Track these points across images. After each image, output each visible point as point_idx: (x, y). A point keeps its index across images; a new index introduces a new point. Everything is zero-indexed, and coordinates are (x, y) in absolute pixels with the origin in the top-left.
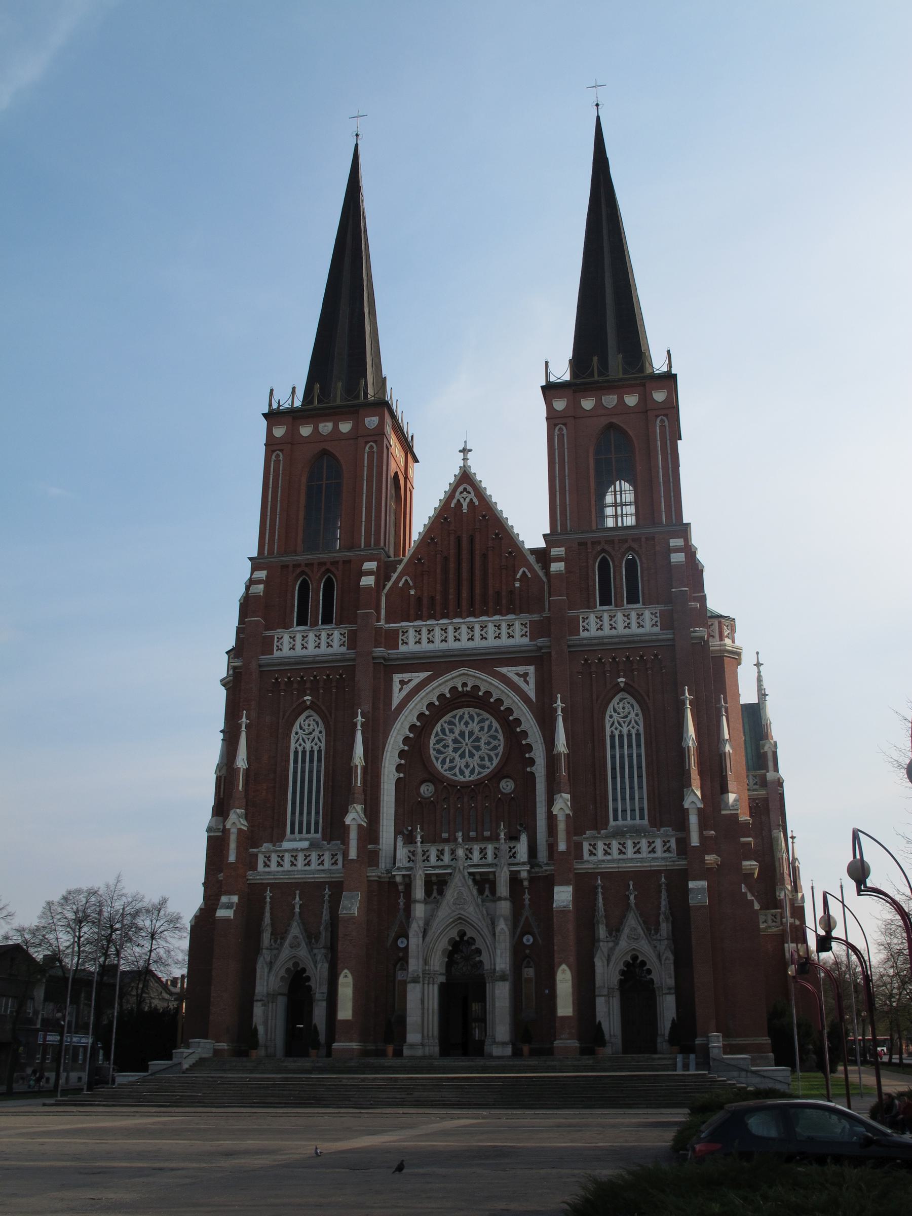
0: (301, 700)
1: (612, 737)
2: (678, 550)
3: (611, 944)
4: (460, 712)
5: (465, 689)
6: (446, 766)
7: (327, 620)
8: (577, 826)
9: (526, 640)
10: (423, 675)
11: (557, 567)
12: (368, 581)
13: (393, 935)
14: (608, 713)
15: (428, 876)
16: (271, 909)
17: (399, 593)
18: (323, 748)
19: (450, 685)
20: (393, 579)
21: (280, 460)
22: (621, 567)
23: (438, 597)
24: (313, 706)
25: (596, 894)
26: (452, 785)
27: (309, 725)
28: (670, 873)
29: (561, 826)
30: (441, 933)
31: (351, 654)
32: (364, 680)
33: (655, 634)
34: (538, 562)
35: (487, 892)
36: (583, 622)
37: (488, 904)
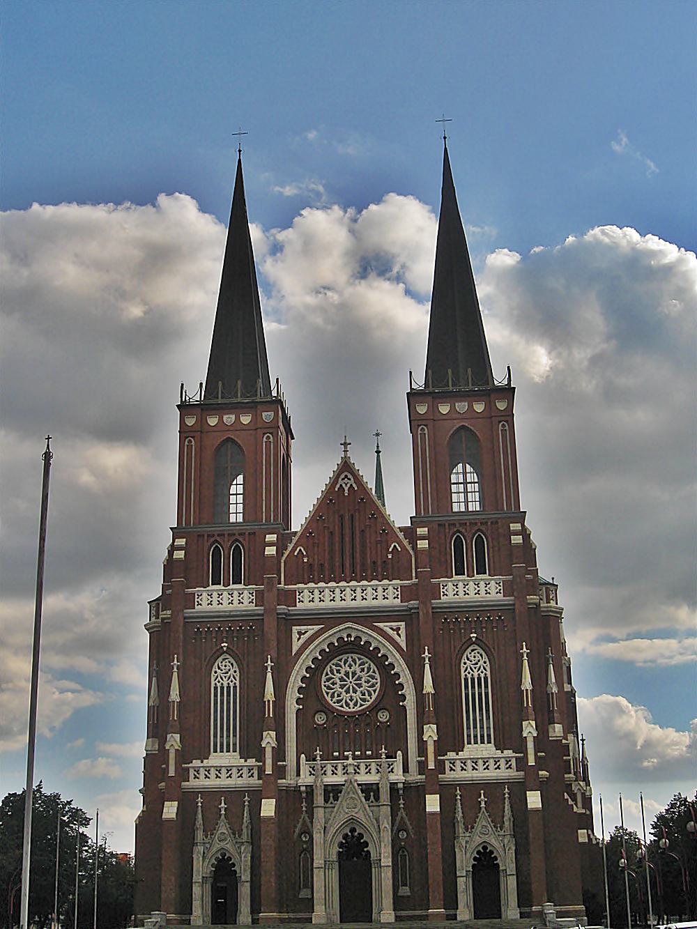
4: (345, 657)
8: (441, 749)
10: (317, 628)
12: (271, 551)
13: (297, 831)
16: (202, 811)
17: (294, 560)
18: (238, 685)
19: (338, 636)
20: (290, 549)
24: (229, 651)
29: (431, 749)
36: (443, 588)
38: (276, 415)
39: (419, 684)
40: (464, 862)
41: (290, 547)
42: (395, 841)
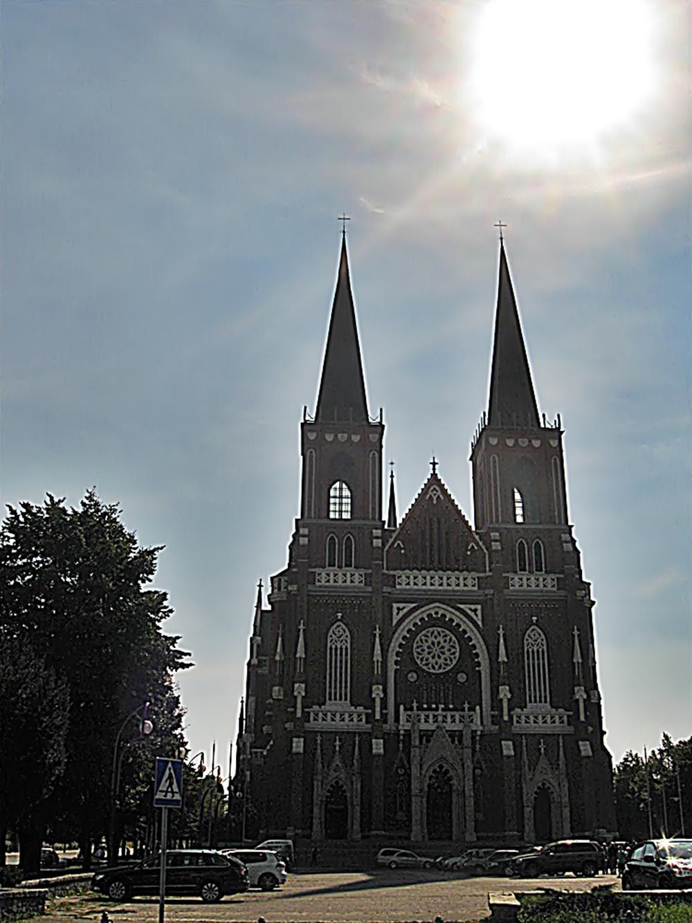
11: (496, 546)
12: (377, 543)
20: (390, 542)
27: (339, 631)
35: (456, 742)
41: (391, 541)
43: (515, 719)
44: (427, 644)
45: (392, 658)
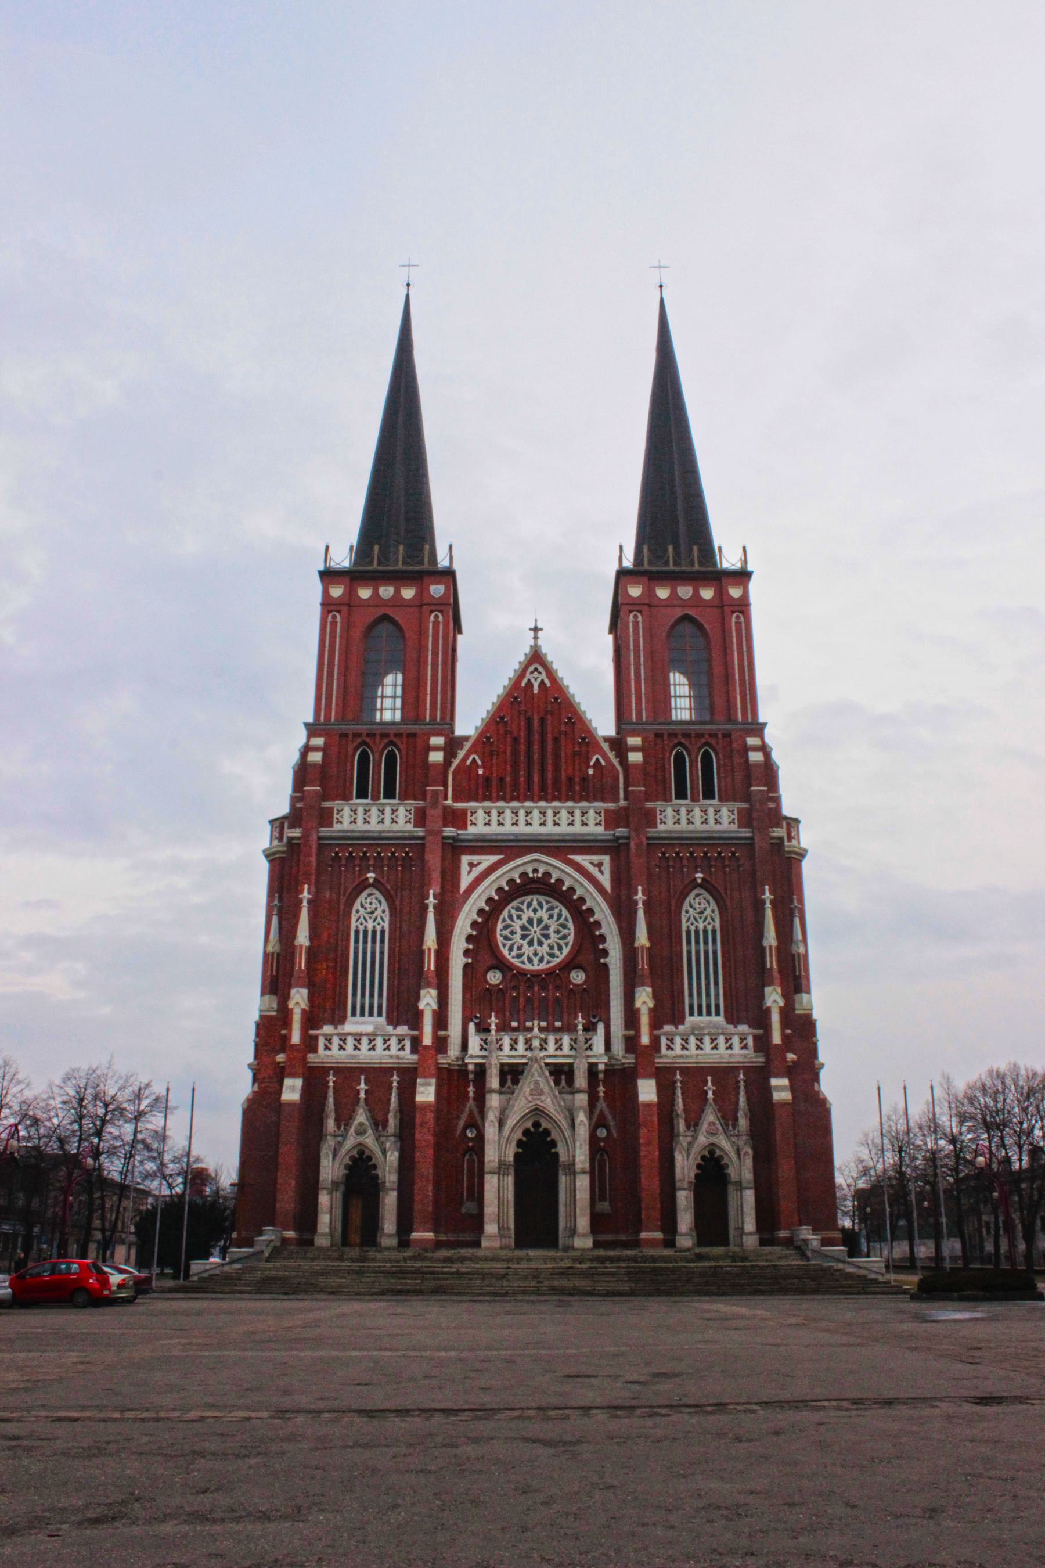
0: (363, 878)
1: (688, 932)
2: (755, 749)
3: (689, 1139)
4: (528, 898)
5: (535, 875)
6: (514, 953)
7: (390, 794)
9: (600, 829)
10: (493, 859)
12: (436, 757)
13: (461, 1123)
14: (684, 909)
15: (502, 1065)
16: (334, 1093)
17: (466, 772)
19: (521, 870)
21: (336, 622)
22: (697, 762)
23: (508, 779)
24: (377, 884)
25: (675, 1088)
26: (522, 973)
28: (748, 1070)
29: (645, 1020)
30: (516, 1124)
31: (420, 831)
32: (434, 860)
33: (734, 832)
34: (612, 749)
35: (563, 1083)
37: (566, 1096)
38: (447, 589)
39: (627, 935)
40: (685, 1166)
42: (593, 1140)
43: (664, 1041)
44: (520, 923)
45: (458, 946)
